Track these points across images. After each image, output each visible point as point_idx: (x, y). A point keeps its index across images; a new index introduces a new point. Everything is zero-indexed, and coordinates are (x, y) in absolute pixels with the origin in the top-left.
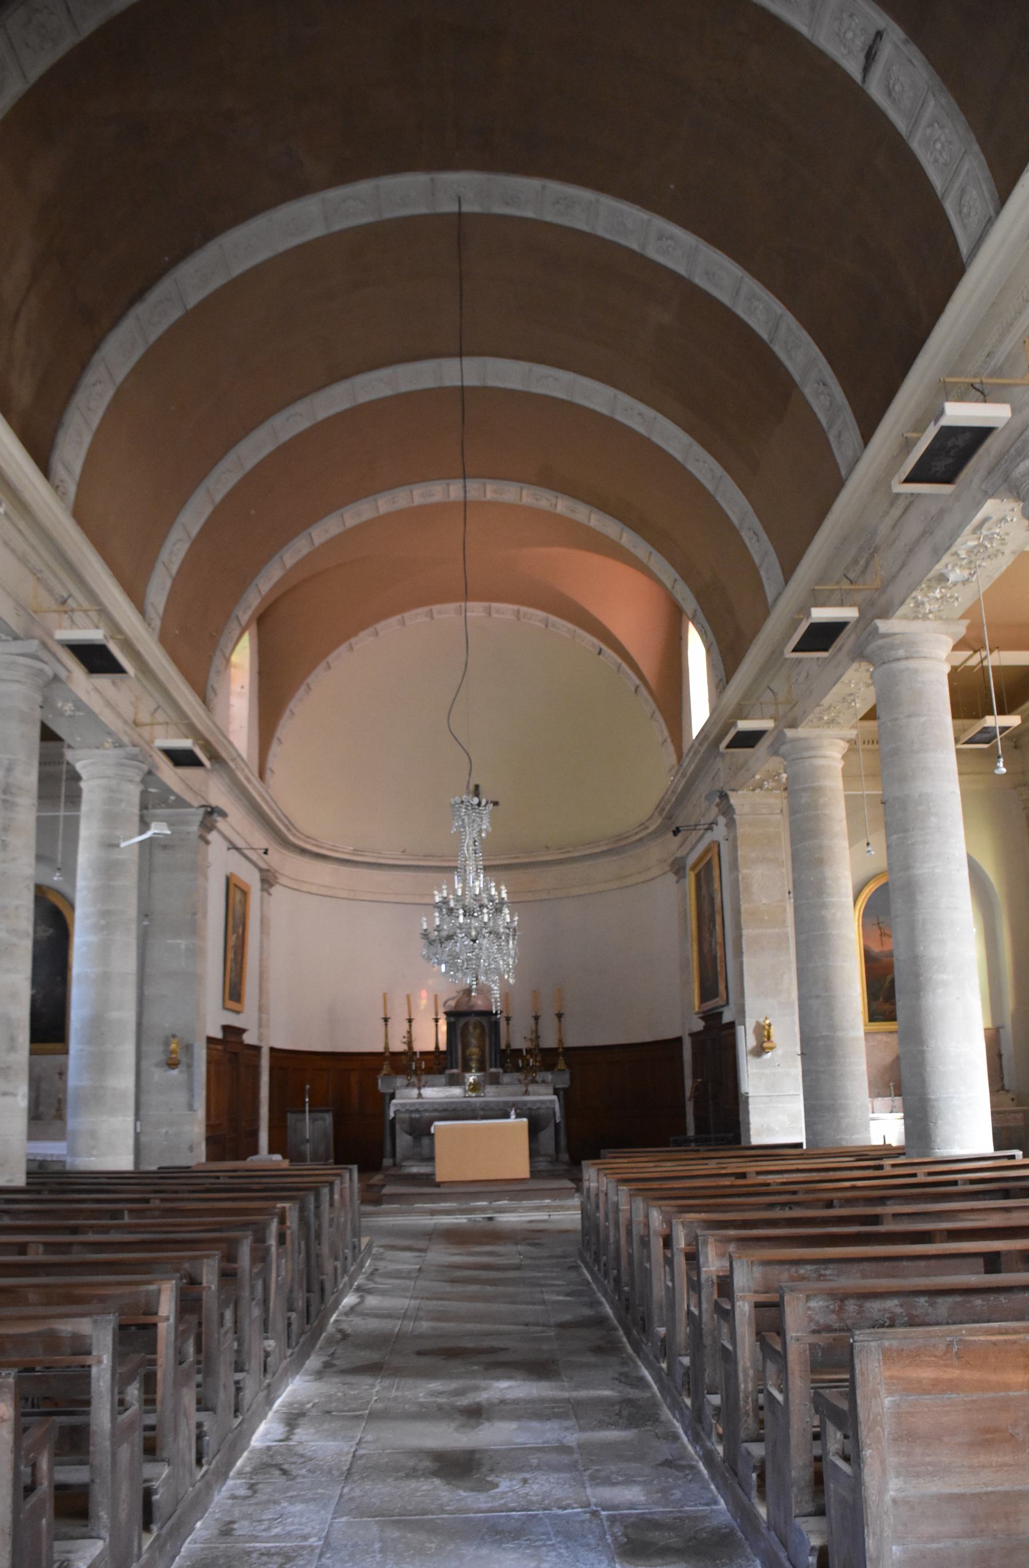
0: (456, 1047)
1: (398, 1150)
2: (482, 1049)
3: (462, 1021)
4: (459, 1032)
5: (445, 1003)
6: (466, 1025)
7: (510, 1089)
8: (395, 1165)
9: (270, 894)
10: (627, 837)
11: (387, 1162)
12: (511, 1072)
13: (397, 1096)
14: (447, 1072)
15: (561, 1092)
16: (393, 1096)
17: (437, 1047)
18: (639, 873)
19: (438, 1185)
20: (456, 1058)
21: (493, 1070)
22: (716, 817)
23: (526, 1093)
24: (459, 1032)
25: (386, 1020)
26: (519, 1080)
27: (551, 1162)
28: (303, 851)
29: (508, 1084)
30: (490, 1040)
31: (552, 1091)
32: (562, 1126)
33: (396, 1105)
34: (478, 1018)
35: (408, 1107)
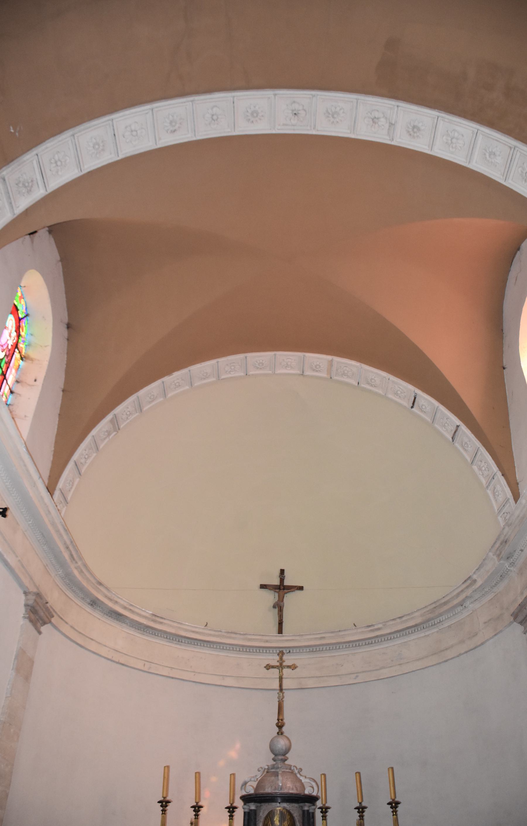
3: (265, 809)
5: (245, 784)
6: (270, 816)
9: (40, 633)
10: (445, 603)
18: (462, 642)
25: (164, 804)
28: (94, 603)
34: (285, 805)
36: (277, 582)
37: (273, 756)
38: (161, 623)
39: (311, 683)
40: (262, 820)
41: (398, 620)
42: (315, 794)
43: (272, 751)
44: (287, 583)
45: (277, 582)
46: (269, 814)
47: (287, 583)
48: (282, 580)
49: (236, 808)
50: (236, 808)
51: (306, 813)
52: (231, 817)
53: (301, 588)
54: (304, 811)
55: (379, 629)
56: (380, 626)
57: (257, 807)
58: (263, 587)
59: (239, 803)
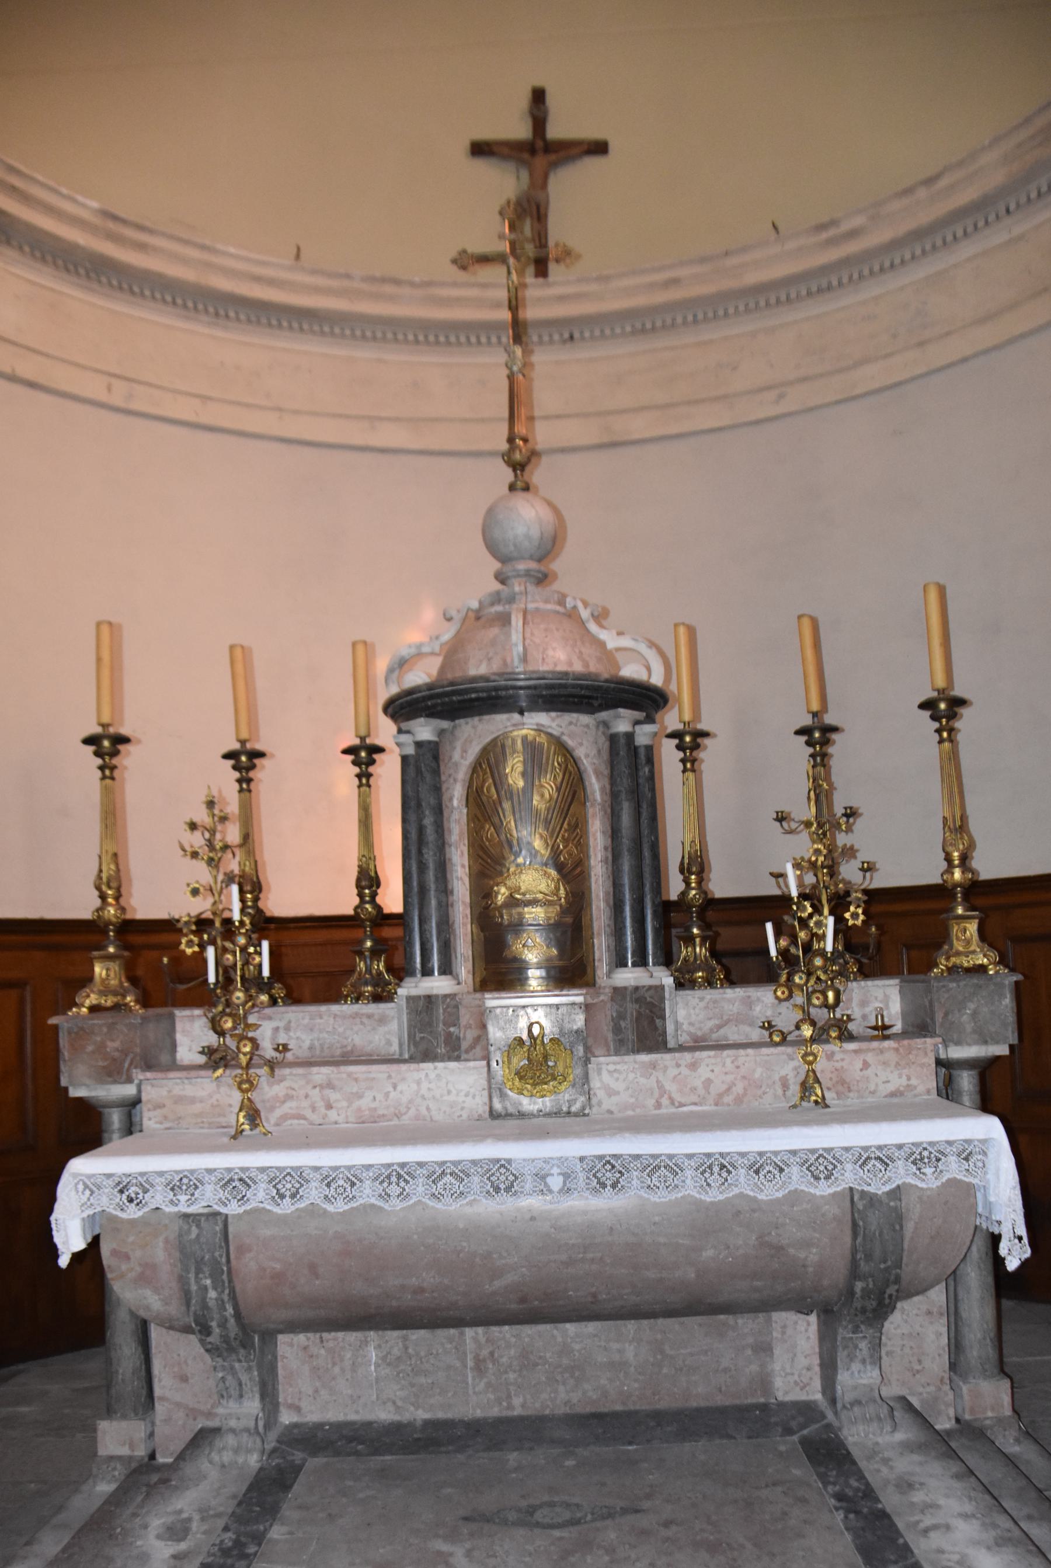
0: (443, 867)
2: (571, 871)
3: (473, 735)
4: (456, 795)
6: (490, 760)
7: (712, 1067)
12: (710, 983)
14: (404, 991)
17: (368, 881)
20: (445, 925)
21: (629, 977)
23: (811, 1098)
24: (456, 795)
26: (769, 1026)
29: (698, 1044)
30: (614, 833)
31: (926, 1081)
33: (91, 1185)
34: (542, 718)
35: (158, 1198)
36: (522, 131)
37: (497, 565)
38: (142, 247)
39: (639, 426)
40: (462, 773)
41: (922, 193)
42: (657, 680)
43: (492, 547)
44: (555, 131)
45: (522, 131)
46: (485, 751)
47: (555, 131)
48: (539, 123)
49: (380, 750)
50: (380, 750)
51: (622, 741)
52: (364, 777)
53: (600, 148)
54: (613, 739)
55: (853, 234)
56: (858, 221)
57: (441, 733)
58: (480, 149)
59: (385, 732)
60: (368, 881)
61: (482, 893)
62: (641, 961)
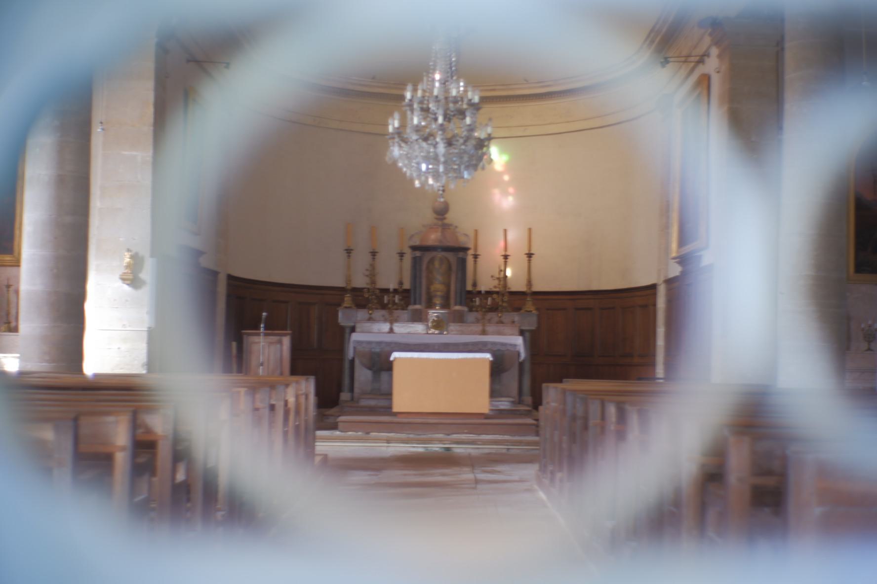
1: (357, 385)
2: (448, 286)
3: (428, 256)
5: (412, 236)
6: (432, 261)
8: (352, 399)
11: (345, 396)
13: (358, 329)
14: (411, 307)
15: (527, 334)
16: (353, 329)
17: (401, 283)
19: (396, 414)
21: (458, 308)
22: (709, 47)
24: (424, 267)
25: (349, 251)
27: (513, 402)
32: (527, 367)
59: (408, 251)
60: (401, 283)
61: (428, 288)
62: (461, 304)
